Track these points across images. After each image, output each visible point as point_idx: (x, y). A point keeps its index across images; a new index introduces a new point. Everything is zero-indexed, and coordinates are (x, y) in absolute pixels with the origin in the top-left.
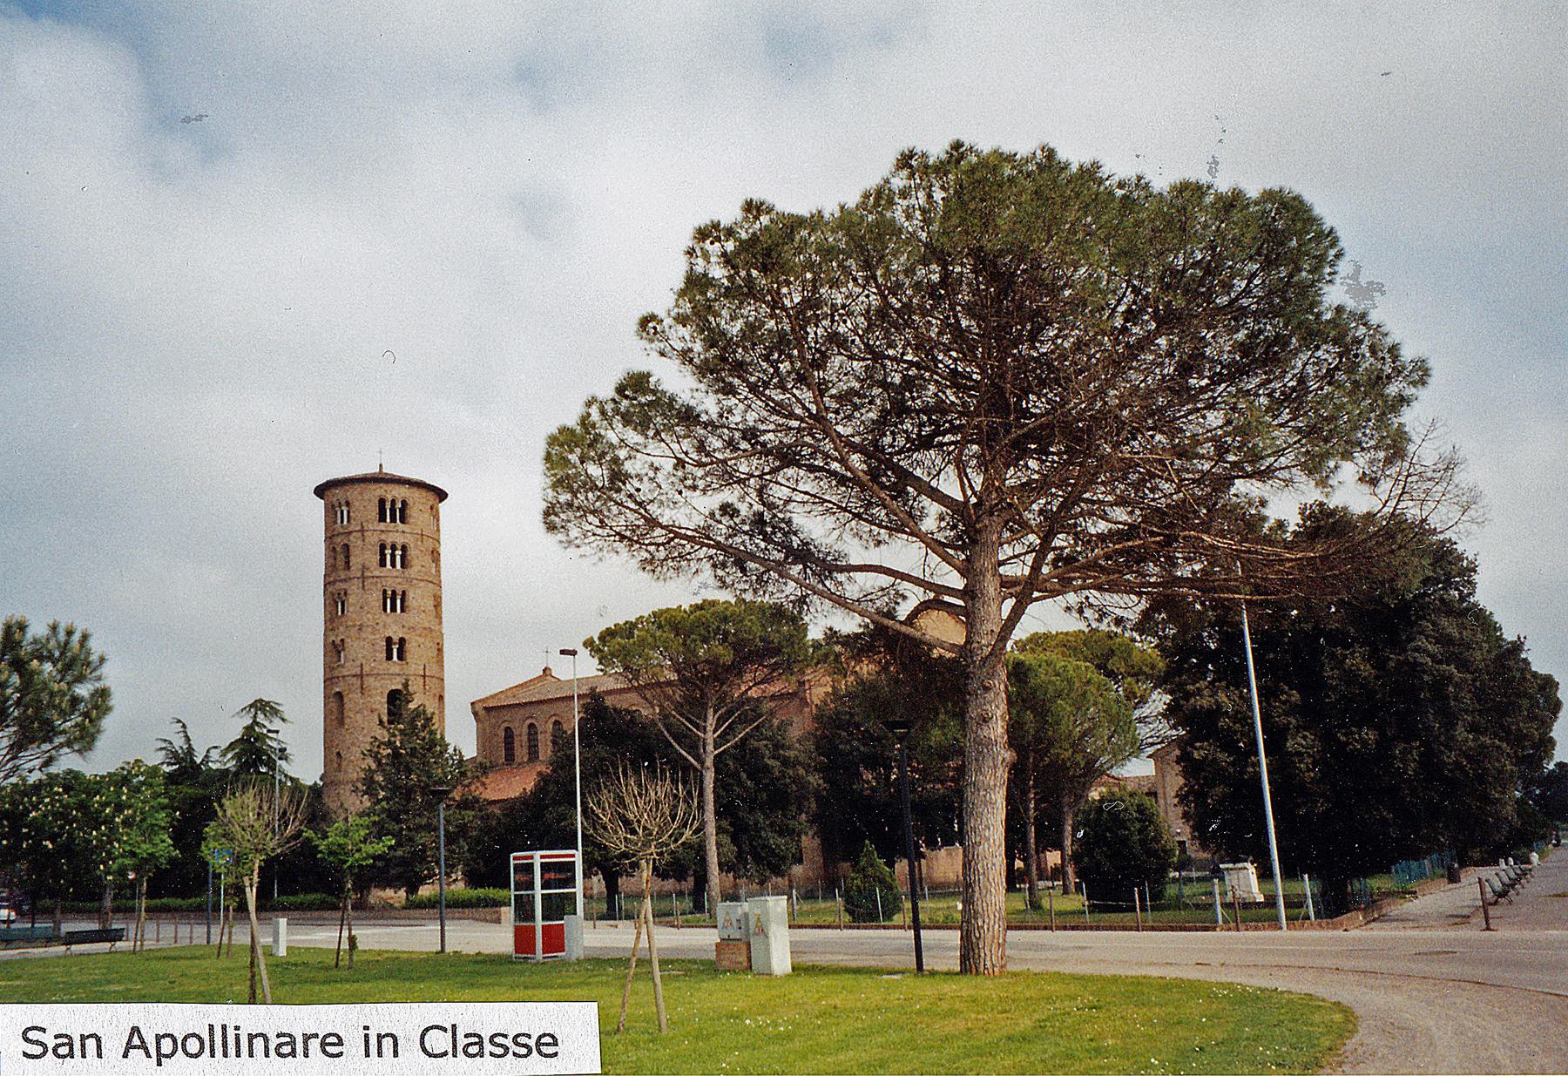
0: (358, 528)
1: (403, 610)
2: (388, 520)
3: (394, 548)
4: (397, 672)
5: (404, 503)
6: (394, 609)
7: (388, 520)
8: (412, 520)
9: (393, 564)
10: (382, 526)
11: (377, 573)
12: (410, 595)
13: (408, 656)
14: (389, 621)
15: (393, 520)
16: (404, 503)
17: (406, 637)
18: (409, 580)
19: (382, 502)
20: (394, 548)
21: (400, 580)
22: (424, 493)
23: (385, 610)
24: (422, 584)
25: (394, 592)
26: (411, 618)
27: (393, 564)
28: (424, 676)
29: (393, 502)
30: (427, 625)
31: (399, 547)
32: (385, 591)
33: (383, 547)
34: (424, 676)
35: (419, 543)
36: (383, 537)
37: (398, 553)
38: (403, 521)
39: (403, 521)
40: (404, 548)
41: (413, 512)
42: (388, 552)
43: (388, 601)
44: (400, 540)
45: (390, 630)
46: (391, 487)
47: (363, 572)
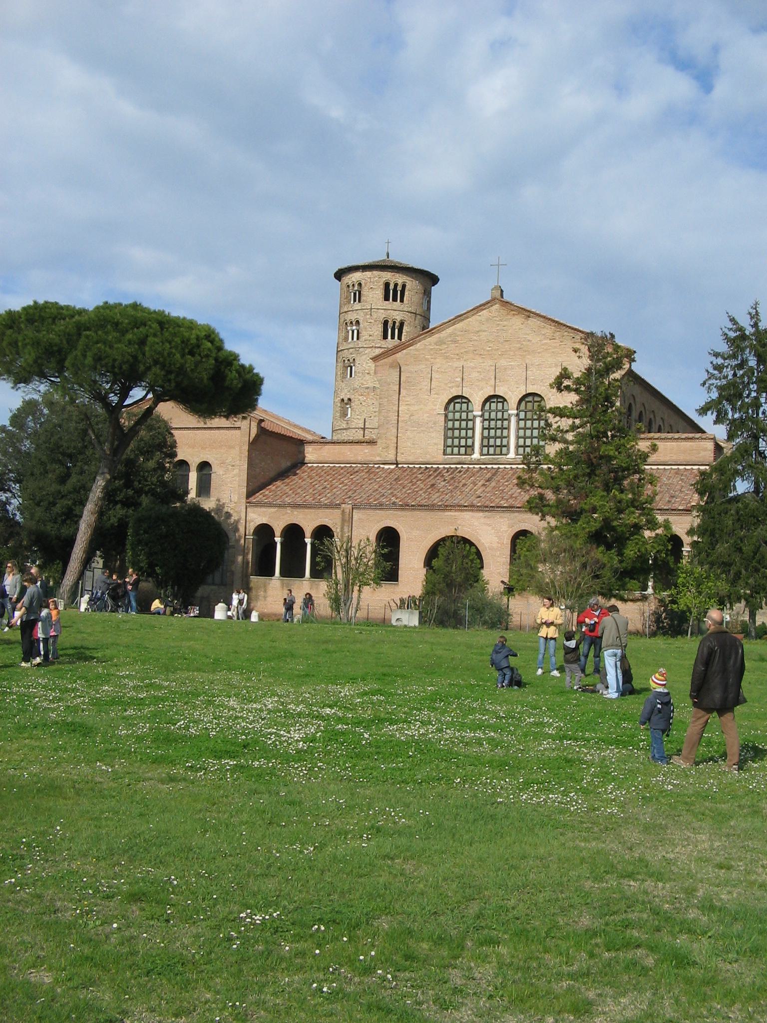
6: (351, 376)
7: (352, 302)
9: (353, 339)
17: (352, 397)
21: (351, 350)
27: (353, 339)
28: (364, 429)
34: (364, 429)
38: (359, 301)
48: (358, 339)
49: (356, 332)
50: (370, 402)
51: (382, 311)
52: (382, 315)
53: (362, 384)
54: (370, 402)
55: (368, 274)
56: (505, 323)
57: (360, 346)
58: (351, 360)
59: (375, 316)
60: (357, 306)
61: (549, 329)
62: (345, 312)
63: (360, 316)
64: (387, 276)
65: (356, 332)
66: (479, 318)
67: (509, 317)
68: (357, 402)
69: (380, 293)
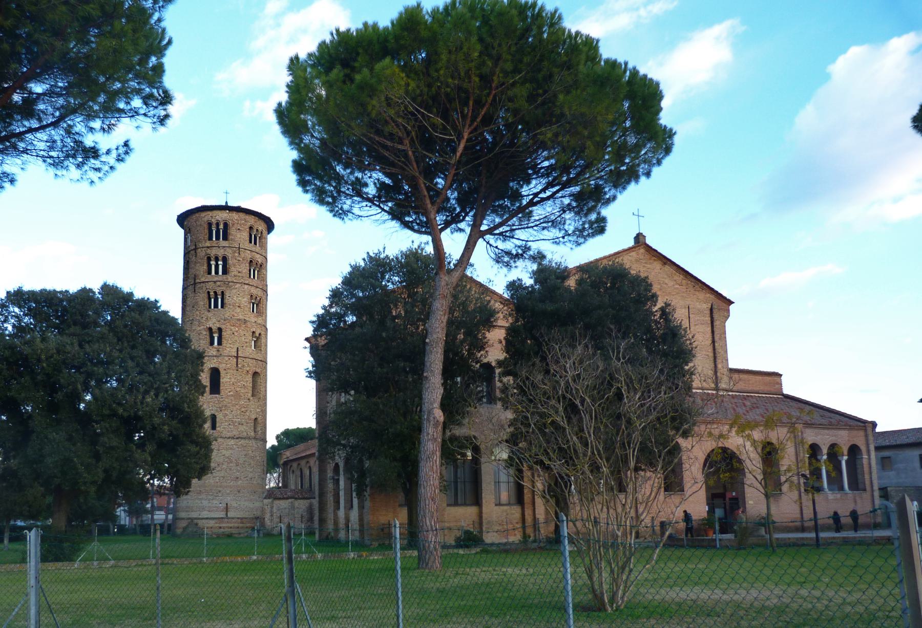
0: (193, 247)
1: (222, 307)
2: (214, 239)
3: (217, 259)
4: (215, 353)
5: (226, 225)
6: (216, 306)
7: (214, 239)
8: (231, 237)
9: (217, 272)
10: (208, 244)
11: (203, 280)
12: (227, 295)
13: (224, 342)
14: (210, 315)
15: (218, 238)
16: (226, 225)
17: (223, 327)
18: (227, 284)
19: (210, 225)
20: (217, 259)
21: (218, 283)
22: (242, 215)
23: (210, 307)
24: (238, 286)
25: (215, 293)
26: (227, 313)
27: (217, 272)
28: (237, 357)
29: (218, 224)
30: (241, 317)
31: (220, 258)
32: (209, 293)
33: (209, 259)
34: (237, 357)
35: (236, 254)
36: (209, 251)
37: (220, 262)
38: (225, 238)
39: (225, 238)
40: (225, 259)
41: (232, 231)
42: (213, 263)
43: (213, 300)
44: (221, 253)
45: (210, 323)
46: (215, 213)
47: (195, 280)
48: (225, 272)
49: (220, 267)
50: (242, 333)
51: (249, 252)
52: (248, 255)
53: (233, 316)
54: (242, 333)
55: (235, 215)
56: (649, 266)
57: (230, 280)
58: (219, 293)
59: (242, 255)
60: (222, 243)
61: (679, 277)
62: (208, 247)
63: (229, 253)
64: (251, 220)
65: (220, 267)
66: (630, 258)
67: (651, 261)
68: (229, 332)
69: (246, 235)
